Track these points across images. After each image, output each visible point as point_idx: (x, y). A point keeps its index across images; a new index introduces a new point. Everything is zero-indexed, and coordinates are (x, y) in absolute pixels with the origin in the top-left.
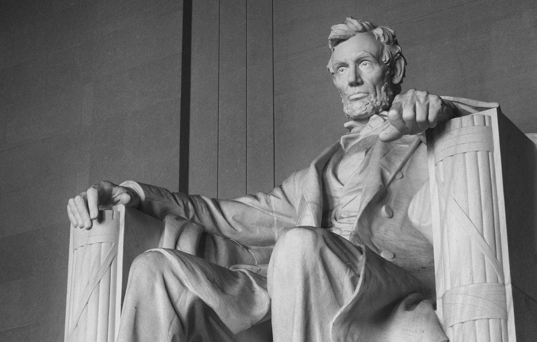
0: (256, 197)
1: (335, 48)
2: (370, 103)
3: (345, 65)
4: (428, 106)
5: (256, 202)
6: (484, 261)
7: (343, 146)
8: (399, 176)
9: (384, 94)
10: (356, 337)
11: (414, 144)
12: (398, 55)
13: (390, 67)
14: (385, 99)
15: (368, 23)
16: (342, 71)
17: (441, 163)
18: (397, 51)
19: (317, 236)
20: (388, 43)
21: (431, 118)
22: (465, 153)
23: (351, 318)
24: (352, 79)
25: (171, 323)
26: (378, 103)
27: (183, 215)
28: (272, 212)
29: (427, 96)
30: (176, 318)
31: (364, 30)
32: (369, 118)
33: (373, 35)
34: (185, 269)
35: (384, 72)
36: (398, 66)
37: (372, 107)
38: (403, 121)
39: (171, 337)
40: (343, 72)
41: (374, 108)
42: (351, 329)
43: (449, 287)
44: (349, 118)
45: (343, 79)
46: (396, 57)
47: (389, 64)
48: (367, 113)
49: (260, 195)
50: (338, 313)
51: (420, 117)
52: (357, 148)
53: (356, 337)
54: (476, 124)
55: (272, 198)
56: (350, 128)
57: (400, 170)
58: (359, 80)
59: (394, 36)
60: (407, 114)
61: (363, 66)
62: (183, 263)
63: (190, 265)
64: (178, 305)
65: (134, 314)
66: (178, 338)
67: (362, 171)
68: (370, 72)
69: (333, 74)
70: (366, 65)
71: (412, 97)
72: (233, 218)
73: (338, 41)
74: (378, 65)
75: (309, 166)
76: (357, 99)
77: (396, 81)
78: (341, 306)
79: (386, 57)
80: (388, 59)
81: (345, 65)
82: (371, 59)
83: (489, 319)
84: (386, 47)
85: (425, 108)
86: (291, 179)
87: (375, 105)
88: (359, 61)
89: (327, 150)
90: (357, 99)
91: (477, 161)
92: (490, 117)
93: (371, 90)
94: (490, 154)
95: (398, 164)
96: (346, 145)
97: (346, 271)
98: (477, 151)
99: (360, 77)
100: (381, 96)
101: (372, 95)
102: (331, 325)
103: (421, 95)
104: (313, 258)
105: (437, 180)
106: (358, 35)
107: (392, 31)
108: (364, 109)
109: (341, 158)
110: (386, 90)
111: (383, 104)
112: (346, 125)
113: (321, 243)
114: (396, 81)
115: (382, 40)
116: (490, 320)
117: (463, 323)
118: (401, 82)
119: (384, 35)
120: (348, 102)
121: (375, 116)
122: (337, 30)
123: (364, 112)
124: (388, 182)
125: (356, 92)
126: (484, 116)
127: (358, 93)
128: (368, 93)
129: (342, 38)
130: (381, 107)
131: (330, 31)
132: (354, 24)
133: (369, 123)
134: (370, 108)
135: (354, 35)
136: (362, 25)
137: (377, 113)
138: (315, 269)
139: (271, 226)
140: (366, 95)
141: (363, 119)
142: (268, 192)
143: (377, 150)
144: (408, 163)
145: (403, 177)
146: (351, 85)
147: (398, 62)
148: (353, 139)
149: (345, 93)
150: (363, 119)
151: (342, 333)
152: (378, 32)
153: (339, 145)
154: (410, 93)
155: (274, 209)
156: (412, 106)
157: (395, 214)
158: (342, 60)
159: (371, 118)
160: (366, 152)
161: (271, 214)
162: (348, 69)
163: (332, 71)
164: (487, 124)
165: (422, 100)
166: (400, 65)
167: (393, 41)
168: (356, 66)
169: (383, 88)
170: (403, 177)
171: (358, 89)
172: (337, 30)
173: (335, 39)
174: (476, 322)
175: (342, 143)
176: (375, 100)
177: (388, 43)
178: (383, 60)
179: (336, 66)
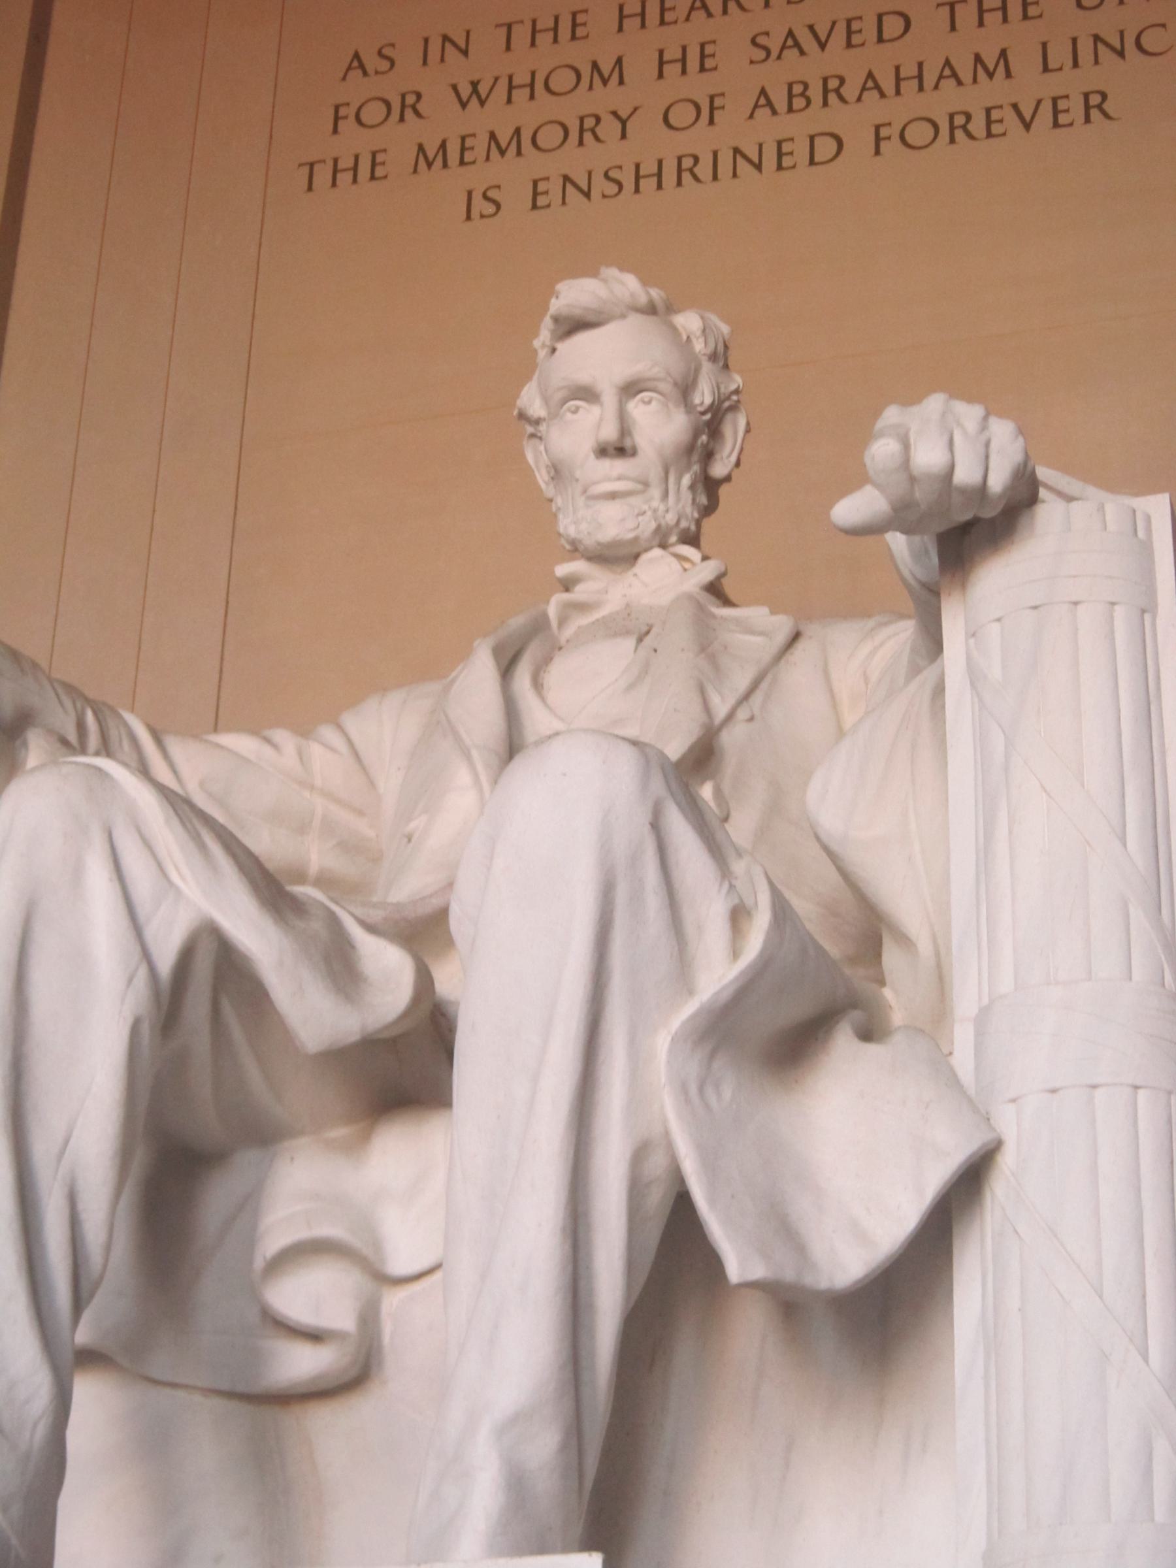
0: (268, 740)
1: (560, 346)
2: (649, 513)
3: (587, 394)
4: (987, 445)
5: (267, 750)
6: (1127, 916)
7: (554, 623)
8: (742, 714)
9: (687, 496)
10: (727, 1093)
11: (781, 638)
12: (735, 398)
13: (708, 424)
14: (689, 510)
15: (662, 294)
16: (576, 411)
17: (996, 627)
18: (733, 387)
19: (648, 762)
20: (713, 357)
21: (998, 481)
22: (1076, 603)
23: (719, 1030)
24: (609, 433)
25: (130, 981)
26: (671, 518)
27: (72, 737)
28: (312, 788)
29: (985, 418)
30: (143, 972)
31: (651, 310)
32: (636, 557)
33: (674, 329)
34: (179, 828)
35: (696, 435)
36: (727, 429)
37: (653, 525)
38: (912, 479)
39: (130, 1021)
40: (575, 417)
41: (659, 527)
42: (717, 1064)
43: (1006, 984)
44: (576, 550)
45: (576, 434)
46: (727, 404)
47: (708, 417)
48: (636, 539)
49: (281, 735)
50: (690, 1008)
51: (966, 475)
52: (614, 628)
53: (727, 1093)
54: (1111, 527)
55: (315, 750)
56: (567, 584)
57: (747, 696)
58: (628, 443)
59: (726, 347)
60: (928, 456)
61: (641, 405)
62: (171, 812)
63: (191, 822)
64: (150, 933)
65: (19, 931)
66: (145, 1029)
67: (631, 687)
68: (659, 426)
69: (537, 422)
70: (649, 402)
71: (943, 415)
72: (202, 784)
73: (574, 325)
74: (682, 409)
75: (462, 654)
76: (613, 496)
77: (719, 470)
78: (691, 992)
79: (704, 396)
80: (708, 400)
81: (587, 394)
82: (665, 387)
83: (1136, 1088)
84: (707, 367)
85: (982, 451)
86: (371, 705)
87: (663, 523)
88: (631, 389)
89: (517, 622)
90: (613, 496)
91: (1112, 632)
92: (1148, 519)
93: (655, 474)
94: (1147, 617)
95: (742, 682)
96: (562, 622)
97: (721, 885)
98: (1113, 604)
99: (630, 434)
100: (678, 500)
101: (656, 492)
102: (662, 1043)
103: (969, 414)
104: (631, 823)
105: (974, 676)
106: (635, 319)
107: (725, 329)
108: (631, 524)
109: (554, 649)
110: (692, 487)
111: (684, 524)
112: (562, 570)
113: (657, 785)
114: (719, 470)
115: (698, 346)
116: (1142, 1094)
117: (1054, 1091)
118: (728, 479)
119: (704, 331)
120: (581, 501)
121: (657, 552)
122: (574, 294)
123: (631, 535)
124: (718, 720)
125: (615, 474)
126: (1134, 511)
127: (619, 478)
128: (646, 484)
129: (591, 318)
130: (676, 531)
131: (551, 292)
132: (626, 285)
133: (637, 569)
134: (648, 526)
135: (623, 316)
136: (648, 293)
137: (663, 546)
138: (634, 859)
139: (302, 829)
140: (640, 487)
141: (618, 557)
142: (304, 730)
143: (678, 638)
144: (764, 685)
145: (751, 719)
146: (602, 451)
147: (729, 417)
148: (582, 607)
149: (578, 474)
150: (618, 557)
151: (693, 1069)
152: (689, 322)
153: (545, 616)
154: (935, 403)
155: (318, 782)
156: (946, 438)
157: (733, 814)
158: (583, 377)
159: (645, 557)
160: (640, 640)
161: (307, 794)
162: (596, 410)
163: (536, 409)
164: (1141, 534)
165: (971, 425)
166: (735, 428)
167: (721, 358)
168: (620, 402)
169: (686, 480)
170: (751, 719)
171: (619, 466)
172: (574, 294)
173: (567, 318)
174: (1098, 1093)
175: (552, 611)
176: (662, 508)
177: (713, 357)
178: (697, 401)
179: (559, 395)
